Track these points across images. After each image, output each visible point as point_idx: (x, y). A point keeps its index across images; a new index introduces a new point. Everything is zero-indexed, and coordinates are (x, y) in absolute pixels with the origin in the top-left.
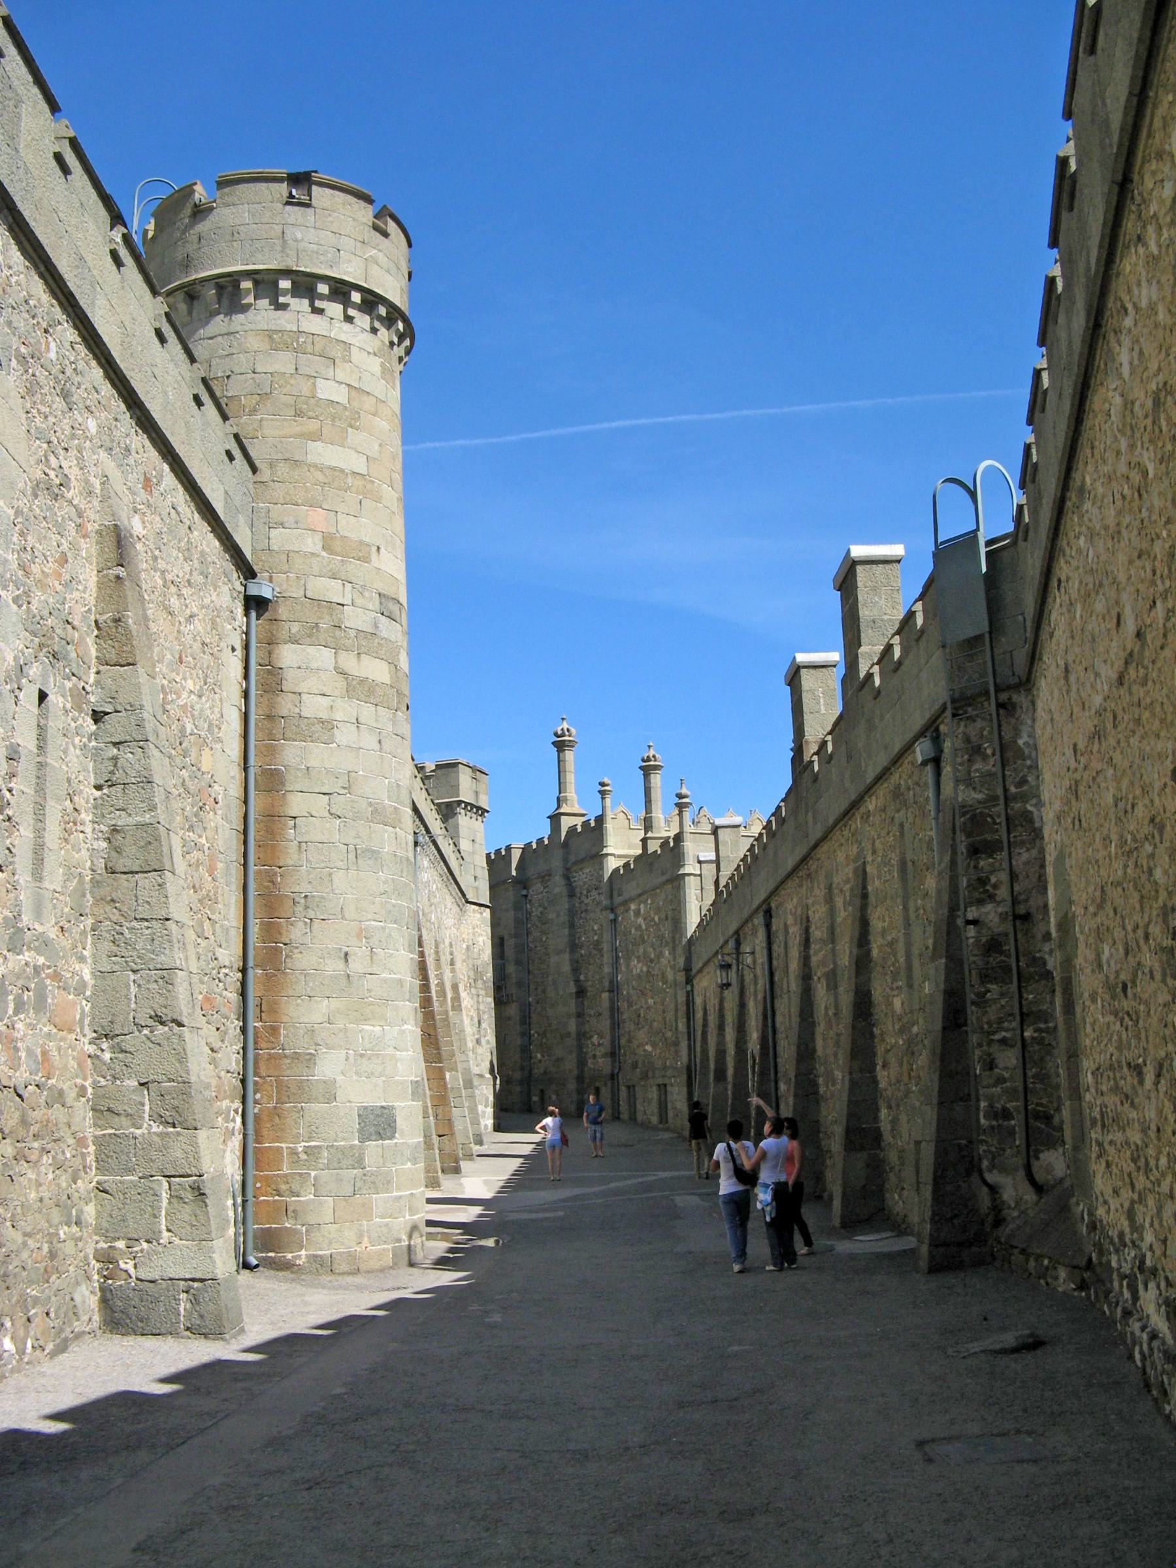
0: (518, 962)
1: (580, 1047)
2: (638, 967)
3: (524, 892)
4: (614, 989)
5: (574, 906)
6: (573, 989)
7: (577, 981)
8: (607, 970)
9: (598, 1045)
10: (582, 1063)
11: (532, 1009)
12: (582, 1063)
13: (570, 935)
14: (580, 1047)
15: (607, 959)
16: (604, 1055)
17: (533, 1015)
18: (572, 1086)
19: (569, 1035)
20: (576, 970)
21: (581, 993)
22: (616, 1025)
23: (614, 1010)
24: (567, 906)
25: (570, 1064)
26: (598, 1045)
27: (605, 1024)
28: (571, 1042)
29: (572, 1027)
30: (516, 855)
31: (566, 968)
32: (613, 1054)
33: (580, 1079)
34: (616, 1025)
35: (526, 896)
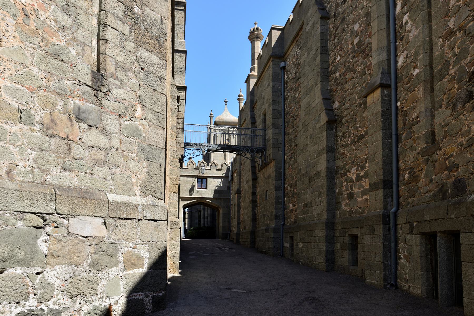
0: (275, 126)
3: (282, 65)
5: (328, 29)
6: (324, 118)
7: (329, 110)
11: (287, 166)
13: (322, 62)
16: (373, 187)
17: (288, 172)
18: (321, 234)
19: (319, 173)
20: (328, 99)
24: (319, 31)
25: (320, 210)
28: (322, 182)
29: (322, 164)
30: (276, 35)
33: (330, 225)
35: (284, 68)
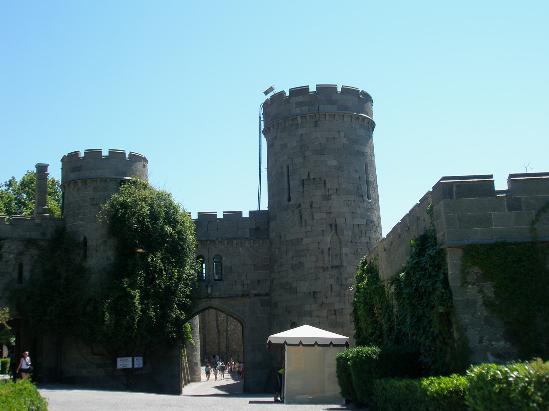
1: (219, 345)
2: (233, 327)
4: (227, 331)
6: (217, 331)
7: (218, 329)
8: (225, 327)
9: (223, 345)
10: (219, 349)
12: (219, 349)
14: (219, 345)
15: (225, 324)
20: (218, 326)
21: (219, 332)
22: (227, 340)
23: (227, 336)
26: (223, 345)
27: (225, 340)
29: (217, 341)
31: (215, 325)
32: (227, 348)
34: (227, 340)
